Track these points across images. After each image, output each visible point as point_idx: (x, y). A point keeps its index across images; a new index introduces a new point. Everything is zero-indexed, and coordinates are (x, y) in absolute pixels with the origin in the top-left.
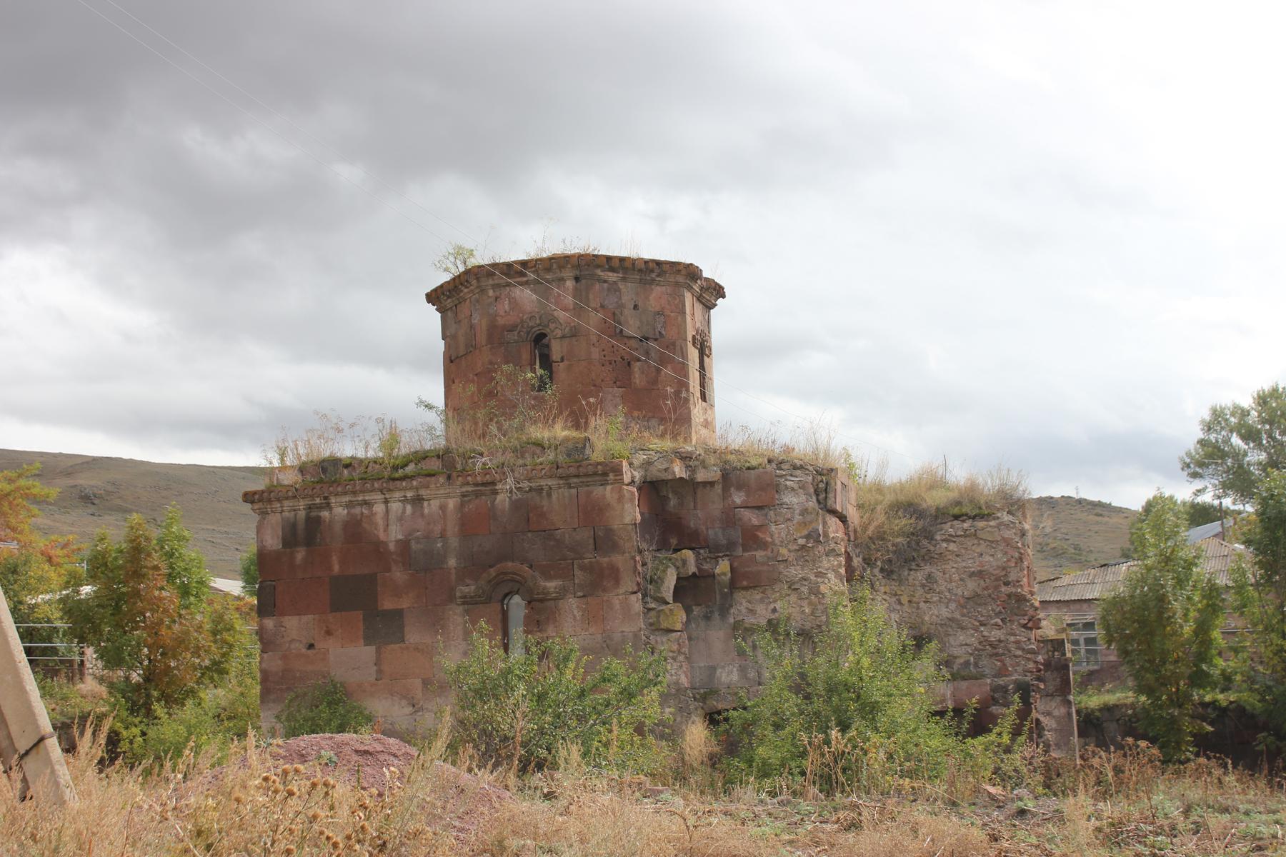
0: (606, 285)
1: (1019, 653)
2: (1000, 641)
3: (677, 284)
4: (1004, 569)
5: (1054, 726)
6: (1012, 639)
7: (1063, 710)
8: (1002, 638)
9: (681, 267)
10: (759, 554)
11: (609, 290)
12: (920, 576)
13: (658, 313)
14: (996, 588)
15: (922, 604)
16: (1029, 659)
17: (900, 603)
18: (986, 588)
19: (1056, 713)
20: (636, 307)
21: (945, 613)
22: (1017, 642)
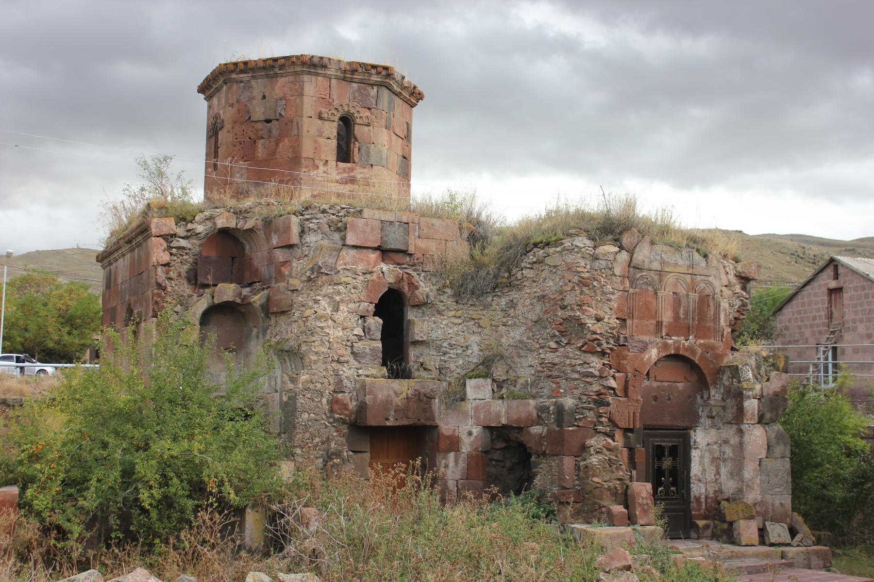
0: (242, 85)
1: (576, 376)
2: (555, 364)
3: (296, 73)
4: (561, 293)
5: (731, 455)
6: (568, 362)
7: (737, 439)
8: (557, 360)
9: (294, 59)
10: (282, 285)
11: (244, 87)
12: (503, 301)
13: (281, 99)
14: (555, 311)
15: (501, 328)
16: (591, 384)
17: (480, 326)
18: (546, 312)
19: (732, 442)
20: (264, 97)
21: (517, 334)
22: (571, 365)
